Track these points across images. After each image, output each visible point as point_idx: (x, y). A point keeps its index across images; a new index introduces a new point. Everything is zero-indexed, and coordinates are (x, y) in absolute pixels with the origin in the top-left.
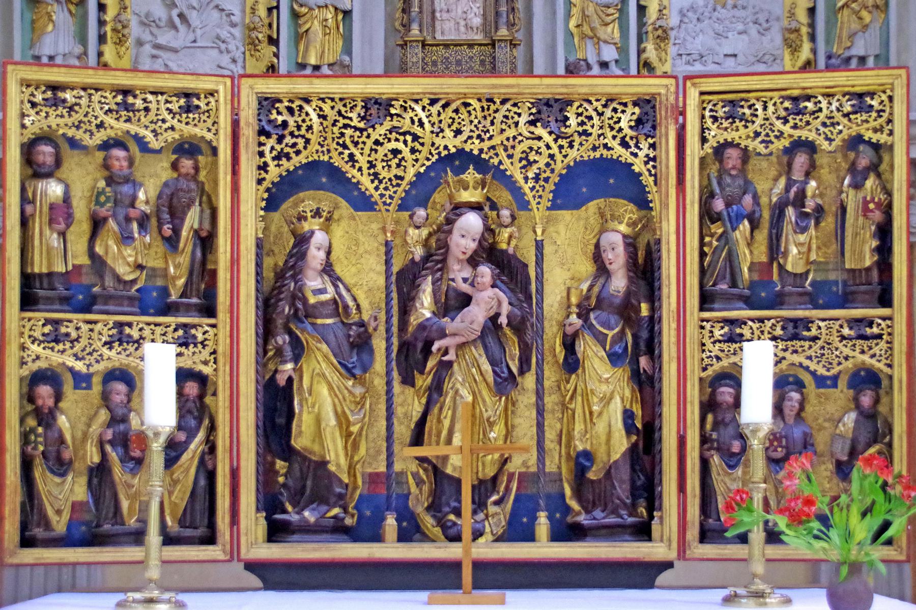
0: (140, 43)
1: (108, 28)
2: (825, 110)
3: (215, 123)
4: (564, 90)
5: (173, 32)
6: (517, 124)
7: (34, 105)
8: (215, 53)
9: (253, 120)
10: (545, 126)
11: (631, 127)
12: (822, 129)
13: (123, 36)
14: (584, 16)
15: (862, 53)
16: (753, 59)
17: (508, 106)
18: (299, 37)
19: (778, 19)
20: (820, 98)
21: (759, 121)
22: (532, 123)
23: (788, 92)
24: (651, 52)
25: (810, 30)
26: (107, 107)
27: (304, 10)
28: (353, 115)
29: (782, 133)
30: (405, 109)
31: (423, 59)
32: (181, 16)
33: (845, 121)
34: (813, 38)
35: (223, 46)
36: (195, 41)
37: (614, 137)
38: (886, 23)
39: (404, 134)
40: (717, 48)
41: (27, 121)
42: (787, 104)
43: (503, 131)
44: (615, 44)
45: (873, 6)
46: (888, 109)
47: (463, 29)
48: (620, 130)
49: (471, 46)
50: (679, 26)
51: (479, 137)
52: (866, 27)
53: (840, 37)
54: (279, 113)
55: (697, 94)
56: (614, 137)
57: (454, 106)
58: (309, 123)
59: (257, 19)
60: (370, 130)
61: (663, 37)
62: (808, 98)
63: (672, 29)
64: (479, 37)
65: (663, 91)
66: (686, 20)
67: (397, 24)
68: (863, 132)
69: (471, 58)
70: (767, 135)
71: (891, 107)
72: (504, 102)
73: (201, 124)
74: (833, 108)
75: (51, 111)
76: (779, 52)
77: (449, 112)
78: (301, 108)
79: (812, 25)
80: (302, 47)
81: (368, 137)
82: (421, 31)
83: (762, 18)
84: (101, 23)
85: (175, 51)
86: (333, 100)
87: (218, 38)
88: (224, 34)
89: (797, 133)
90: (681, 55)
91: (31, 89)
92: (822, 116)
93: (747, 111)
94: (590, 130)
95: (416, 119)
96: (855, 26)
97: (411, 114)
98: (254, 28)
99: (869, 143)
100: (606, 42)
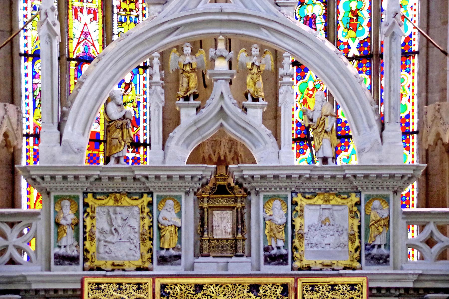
0: (99, 240)
1: (87, 235)
2: (341, 289)
3: (147, 293)
4: (259, 282)
5: (112, 236)
6: (243, 292)
7: (92, 290)
8: (128, 244)
9: (159, 292)
10: (252, 293)
11: (280, 293)
12: (341, 295)
13: (93, 238)
14: (271, 229)
15: (379, 244)
16: (336, 246)
17: (241, 286)
18: (161, 237)
19: (346, 230)
20: (340, 285)
21: (321, 292)
22: (248, 292)
23: (330, 283)
24: (297, 243)
26: (114, 289)
27: (163, 227)
28: (191, 290)
29: (328, 296)
30: (208, 288)
31: (209, 245)
32: (115, 229)
33: (348, 293)
34: (360, 237)
35: (132, 241)
36: (121, 239)
37: (275, 297)
38: (388, 231)
39: (207, 296)
40: (322, 241)
41: (90, 295)
42: (330, 287)
43: (239, 295)
44: (283, 240)
46: (361, 290)
47: (224, 233)
48: (277, 294)
49: (227, 240)
50: (308, 233)
51: (231, 297)
52: (380, 233)
53: (371, 237)
54: (167, 289)
55: (301, 283)
56: (275, 297)
57: (223, 286)
58: (177, 292)
59: (145, 231)
60: (197, 295)
61: (302, 237)
62: (336, 285)
63: (305, 233)
64: (230, 237)
65: (290, 282)
66: (310, 230)
67: (199, 232)
68: (353, 297)
69: (227, 245)
70: (323, 297)
72: (239, 285)
73: (143, 294)
74: (344, 289)
75: (97, 291)
76: (347, 243)
77: (222, 288)
78: (174, 288)
79: (360, 232)
80: (162, 241)
81: (196, 297)
82: (208, 235)
83: (340, 229)
84: (84, 233)
85: (113, 243)
86: (185, 285)
87: (129, 238)
88: (132, 237)
89: (333, 297)
90: (308, 244)
91: (91, 285)
92: (340, 291)
93: (317, 289)
94: (267, 294)
95: (211, 291)
96: (376, 233)
97: (210, 289)
98: (144, 234)
100: (279, 239)
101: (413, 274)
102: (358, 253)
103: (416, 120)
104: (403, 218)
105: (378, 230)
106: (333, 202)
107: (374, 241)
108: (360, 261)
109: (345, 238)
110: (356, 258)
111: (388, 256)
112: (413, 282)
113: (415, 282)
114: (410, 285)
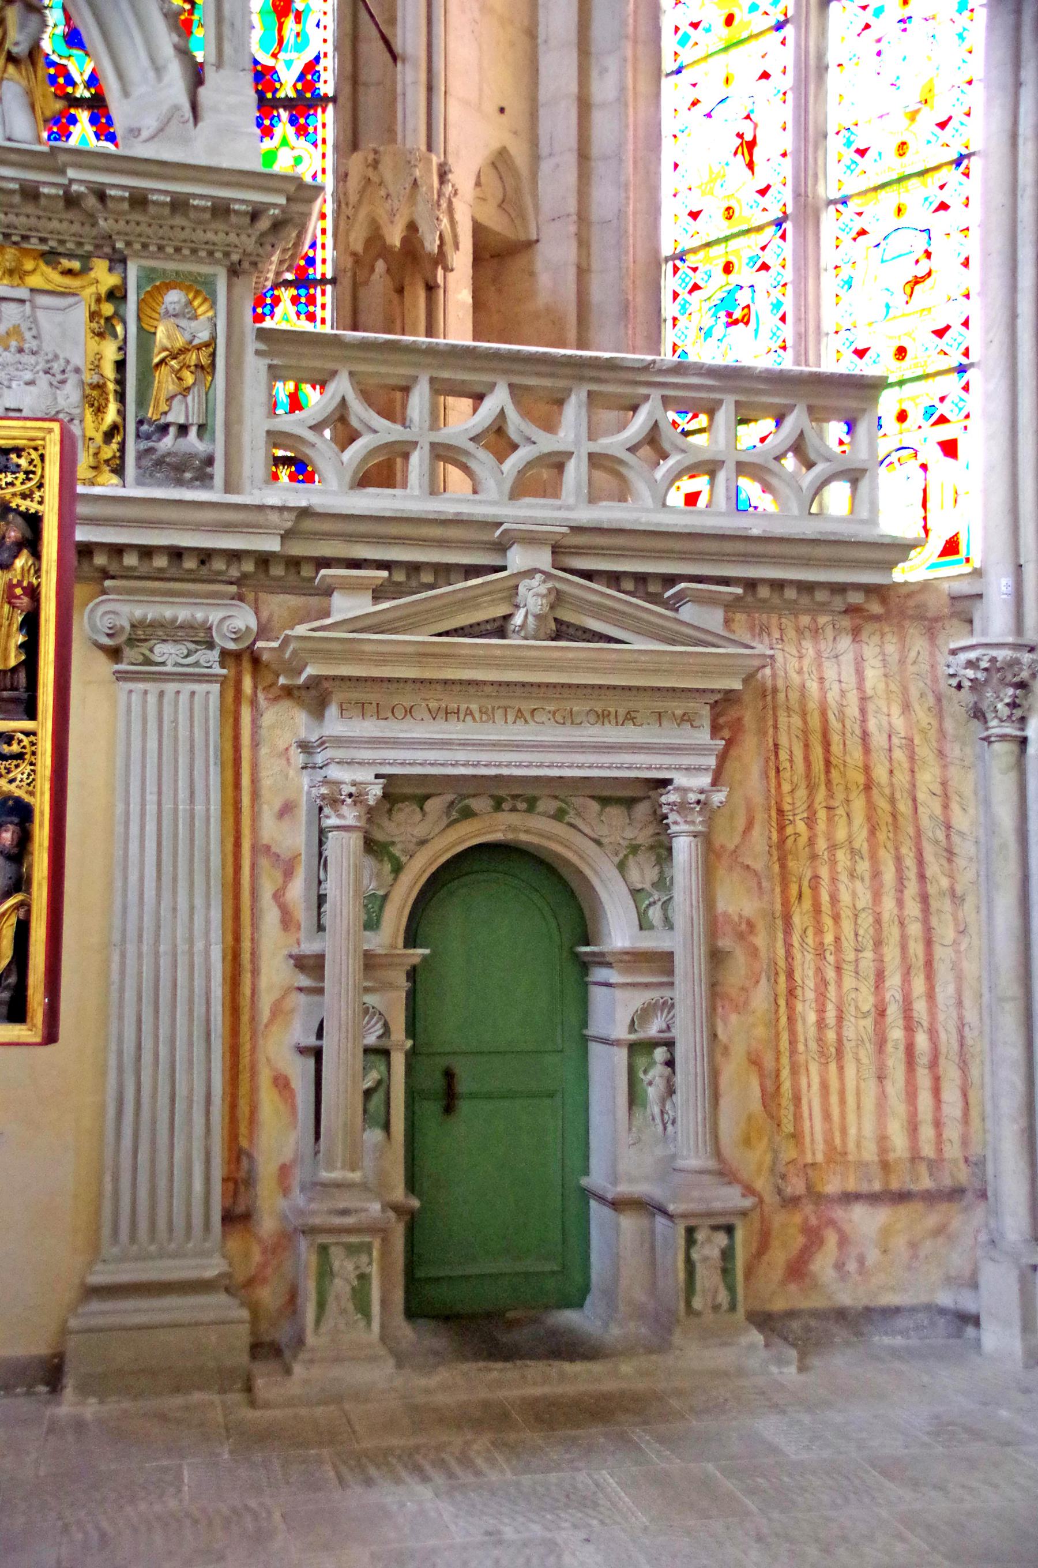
15: (182, 420)
25: (118, 388)
34: (121, 397)
45: (196, 366)
53: (157, 401)
71: (43, 468)
79: (121, 382)
83: (56, 367)
99: (17, 511)
101: (282, 509)
102: (114, 446)
103: (329, 253)
104: (258, 353)
105: (180, 379)
106: (35, 281)
107: (166, 413)
108: (119, 470)
109: (70, 396)
110: (107, 462)
111: (210, 461)
112: (282, 537)
113: (286, 536)
114: (272, 545)
